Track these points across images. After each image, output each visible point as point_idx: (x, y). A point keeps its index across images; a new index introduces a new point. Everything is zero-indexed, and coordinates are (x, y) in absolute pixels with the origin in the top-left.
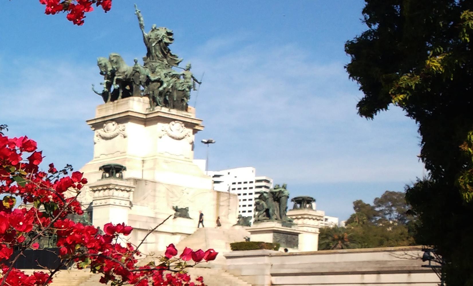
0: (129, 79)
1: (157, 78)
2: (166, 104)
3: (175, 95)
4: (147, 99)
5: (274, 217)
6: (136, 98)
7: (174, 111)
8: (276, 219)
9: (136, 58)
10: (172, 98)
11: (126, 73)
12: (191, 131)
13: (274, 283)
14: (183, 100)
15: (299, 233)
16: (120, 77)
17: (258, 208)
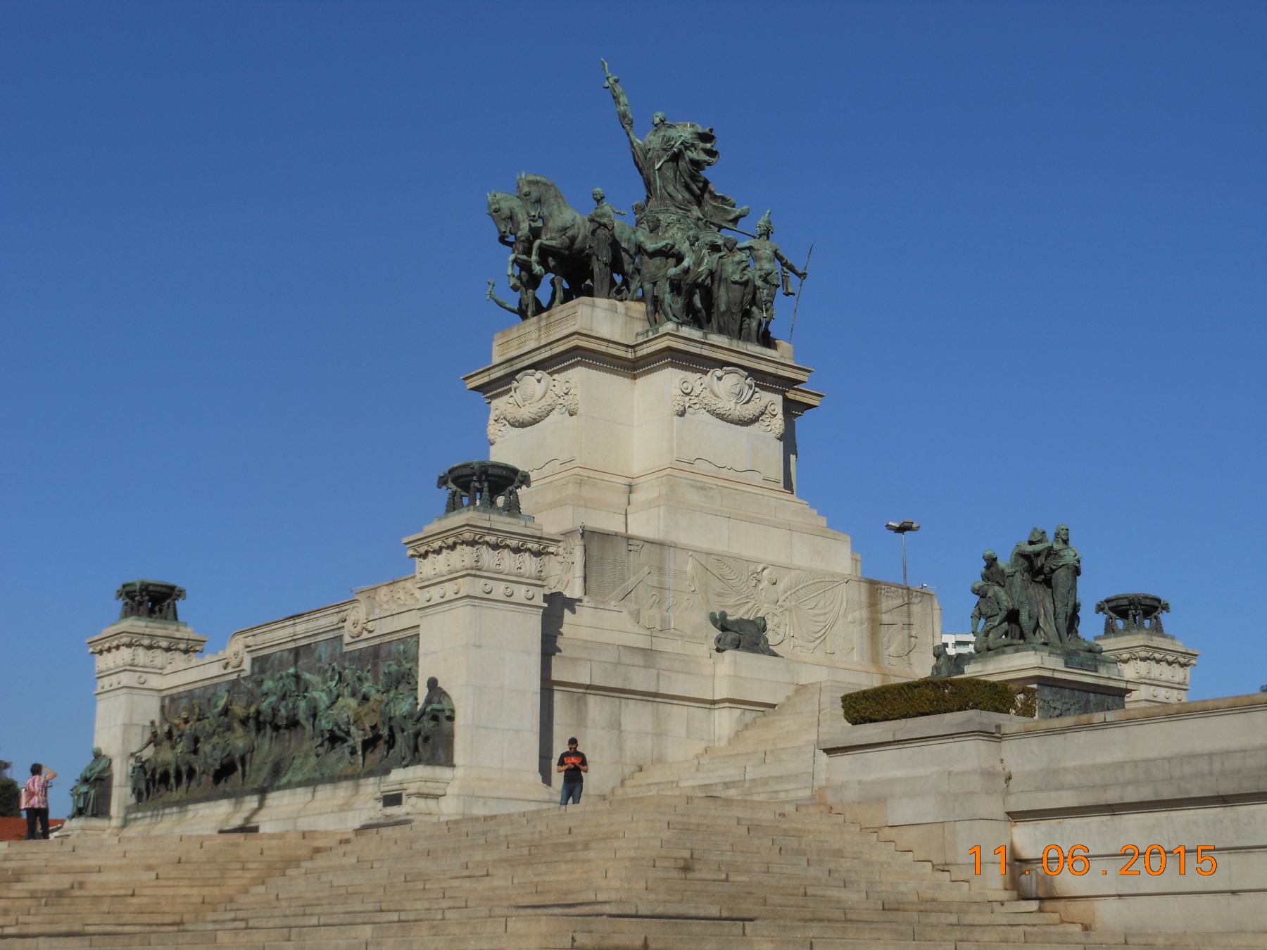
0: (582, 250)
1: (661, 244)
2: (696, 318)
3: (723, 297)
4: (639, 308)
5: (1039, 638)
6: (601, 302)
7: (715, 339)
8: (1045, 644)
9: (598, 190)
10: (715, 308)
11: (570, 233)
12: (779, 398)
13: (1027, 853)
14: (747, 314)
15: (1130, 691)
16: (553, 243)
17: (984, 610)
